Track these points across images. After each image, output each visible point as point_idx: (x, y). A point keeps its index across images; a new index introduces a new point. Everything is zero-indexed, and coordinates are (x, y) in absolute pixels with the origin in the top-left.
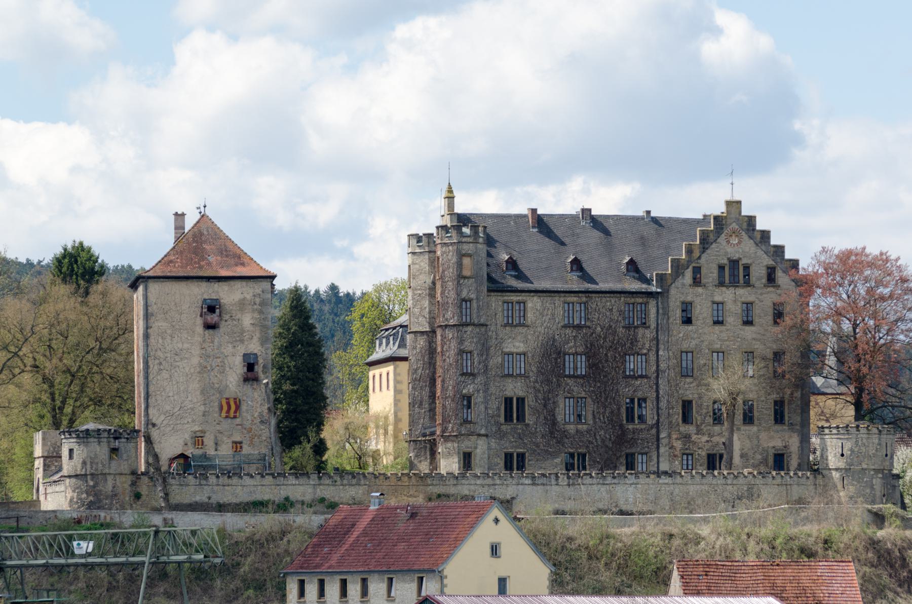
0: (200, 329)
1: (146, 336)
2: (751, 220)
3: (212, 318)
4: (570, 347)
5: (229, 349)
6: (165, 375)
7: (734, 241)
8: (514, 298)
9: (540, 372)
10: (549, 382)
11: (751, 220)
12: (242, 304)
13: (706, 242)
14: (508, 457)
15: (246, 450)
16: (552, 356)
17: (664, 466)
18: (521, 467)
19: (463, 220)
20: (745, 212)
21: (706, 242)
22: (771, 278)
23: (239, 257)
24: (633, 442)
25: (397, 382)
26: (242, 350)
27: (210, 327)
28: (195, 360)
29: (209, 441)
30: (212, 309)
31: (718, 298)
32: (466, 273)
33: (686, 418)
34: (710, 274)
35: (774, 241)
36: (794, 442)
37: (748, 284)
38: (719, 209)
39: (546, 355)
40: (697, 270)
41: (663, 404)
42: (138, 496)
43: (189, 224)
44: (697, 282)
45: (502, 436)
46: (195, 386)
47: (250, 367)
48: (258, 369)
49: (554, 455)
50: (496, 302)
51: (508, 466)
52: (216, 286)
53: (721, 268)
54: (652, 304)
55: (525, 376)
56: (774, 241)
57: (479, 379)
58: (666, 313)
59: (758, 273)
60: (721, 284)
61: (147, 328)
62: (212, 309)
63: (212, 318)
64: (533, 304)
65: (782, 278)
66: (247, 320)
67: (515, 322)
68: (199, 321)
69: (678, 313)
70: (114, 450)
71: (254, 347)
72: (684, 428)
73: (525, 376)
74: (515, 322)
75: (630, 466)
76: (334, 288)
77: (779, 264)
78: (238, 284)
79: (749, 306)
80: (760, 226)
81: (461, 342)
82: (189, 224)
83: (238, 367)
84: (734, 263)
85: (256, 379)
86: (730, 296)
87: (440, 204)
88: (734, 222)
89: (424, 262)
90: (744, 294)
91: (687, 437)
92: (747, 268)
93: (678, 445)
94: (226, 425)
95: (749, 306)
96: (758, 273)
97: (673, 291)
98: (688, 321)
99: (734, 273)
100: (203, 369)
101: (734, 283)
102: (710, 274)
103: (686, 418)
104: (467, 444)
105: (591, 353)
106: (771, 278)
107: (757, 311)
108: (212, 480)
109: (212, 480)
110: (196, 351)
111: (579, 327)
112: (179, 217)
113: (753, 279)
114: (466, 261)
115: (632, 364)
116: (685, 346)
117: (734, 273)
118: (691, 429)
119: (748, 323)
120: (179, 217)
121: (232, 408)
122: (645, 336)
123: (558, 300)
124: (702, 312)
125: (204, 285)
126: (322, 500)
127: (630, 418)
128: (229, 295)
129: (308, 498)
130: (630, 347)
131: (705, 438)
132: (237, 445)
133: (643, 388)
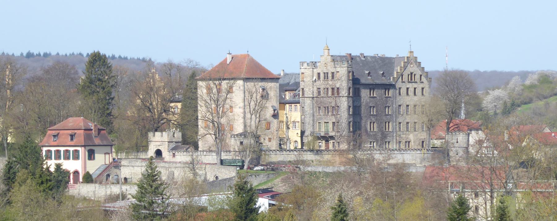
31: (408, 86)
34: (405, 78)
35: (422, 66)
38: (406, 54)
40: (402, 76)
47: (274, 110)
56: (422, 66)
59: (418, 77)
65: (424, 79)
80: (418, 61)
84: (412, 73)
86: (411, 86)
90: (415, 85)
95: (415, 89)
96: (418, 77)
102: (405, 78)
124: (404, 91)
131: (405, 136)
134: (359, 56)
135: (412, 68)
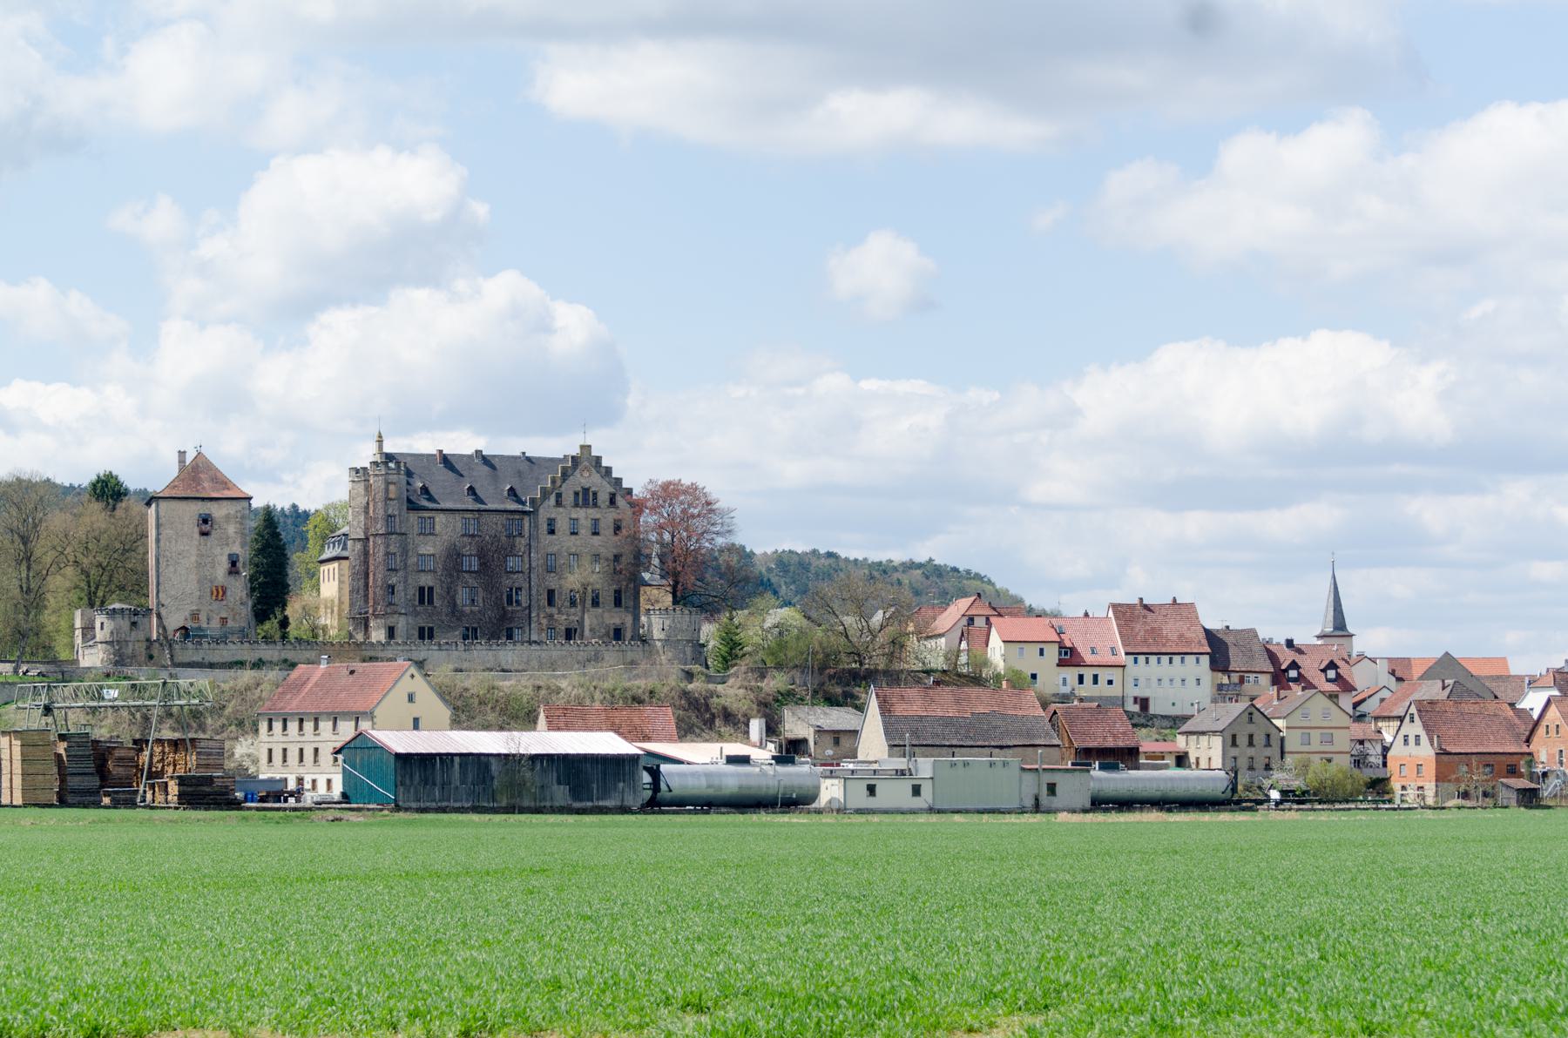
0: (197, 535)
1: (158, 541)
2: (598, 459)
3: (206, 528)
4: (466, 551)
5: (217, 551)
6: (171, 569)
7: (586, 474)
8: (426, 514)
9: (445, 569)
10: (451, 576)
11: (598, 459)
12: (228, 517)
13: (565, 476)
14: (421, 630)
15: (230, 624)
16: (453, 558)
17: (534, 637)
18: (431, 637)
19: (389, 457)
20: (594, 453)
21: (565, 476)
22: (612, 501)
23: (225, 483)
24: (511, 620)
25: (340, 575)
26: (227, 551)
27: (204, 534)
28: (193, 559)
29: (203, 617)
30: (205, 521)
32: (392, 496)
33: (551, 602)
34: (568, 498)
35: (615, 475)
36: (629, 620)
37: (595, 505)
38: (575, 451)
39: (449, 556)
40: (559, 496)
41: (534, 592)
42: (151, 657)
43: (189, 459)
44: (559, 504)
45: (417, 614)
46: (193, 577)
47: (234, 564)
48: (240, 565)
49: (454, 629)
50: (413, 517)
51: (421, 637)
52: (209, 504)
53: (577, 494)
54: (526, 519)
55: (434, 572)
56: (615, 475)
57: (401, 573)
58: (537, 526)
59: (603, 498)
60: (576, 505)
61: (158, 534)
62: (205, 521)
63: (206, 528)
64: (440, 519)
65: (620, 501)
66: (231, 529)
67: (428, 531)
68: (196, 530)
69: (545, 526)
70: (134, 624)
71: (236, 549)
72: (549, 610)
73: (434, 572)
74: (428, 531)
75: (510, 637)
76: (294, 506)
77: (619, 492)
78: (225, 503)
79: (596, 521)
81: (388, 546)
82: (189, 459)
83: (225, 564)
84: (586, 490)
85: (237, 573)
86: (582, 514)
87: (374, 448)
88: (585, 460)
89: (361, 488)
90: (593, 513)
91: (551, 616)
92: (595, 494)
93: (545, 622)
94: (216, 605)
96: (603, 498)
97: (541, 511)
98: (552, 532)
99: (586, 498)
100: (199, 565)
101: (586, 504)
102: (568, 498)
103: (551, 602)
104: (391, 621)
105: (482, 554)
106: (612, 501)
107: (602, 524)
108: (205, 646)
109: (205, 646)
110: (194, 551)
111: (473, 536)
112: (182, 454)
113: (599, 503)
114: (392, 487)
115: (512, 563)
116: (550, 550)
117: (586, 498)
118: (554, 610)
119: (596, 533)
120: (182, 454)
121: (220, 593)
122: (521, 543)
123: (458, 517)
124: (562, 525)
125: (200, 503)
126: (285, 661)
127: (510, 602)
128: (218, 511)
129: (275, 659)
130: (510, 551)
132: (224, 620)
133: (519, 580)
134: (470, 457)
135: (582, 479)
